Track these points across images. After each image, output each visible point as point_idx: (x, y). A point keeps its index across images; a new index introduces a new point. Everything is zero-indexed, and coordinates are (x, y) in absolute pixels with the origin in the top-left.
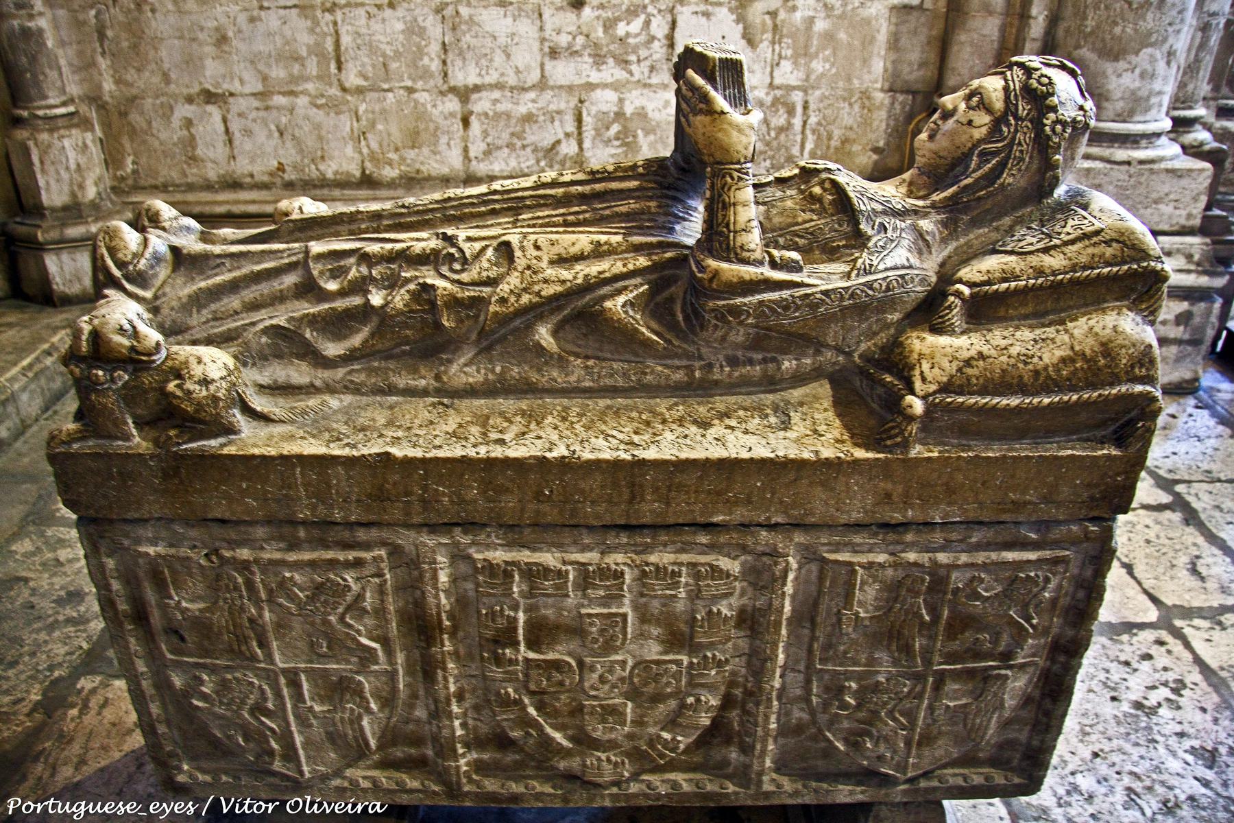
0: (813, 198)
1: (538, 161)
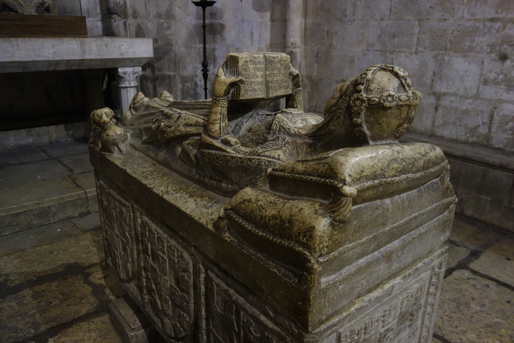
1: (466, 134)
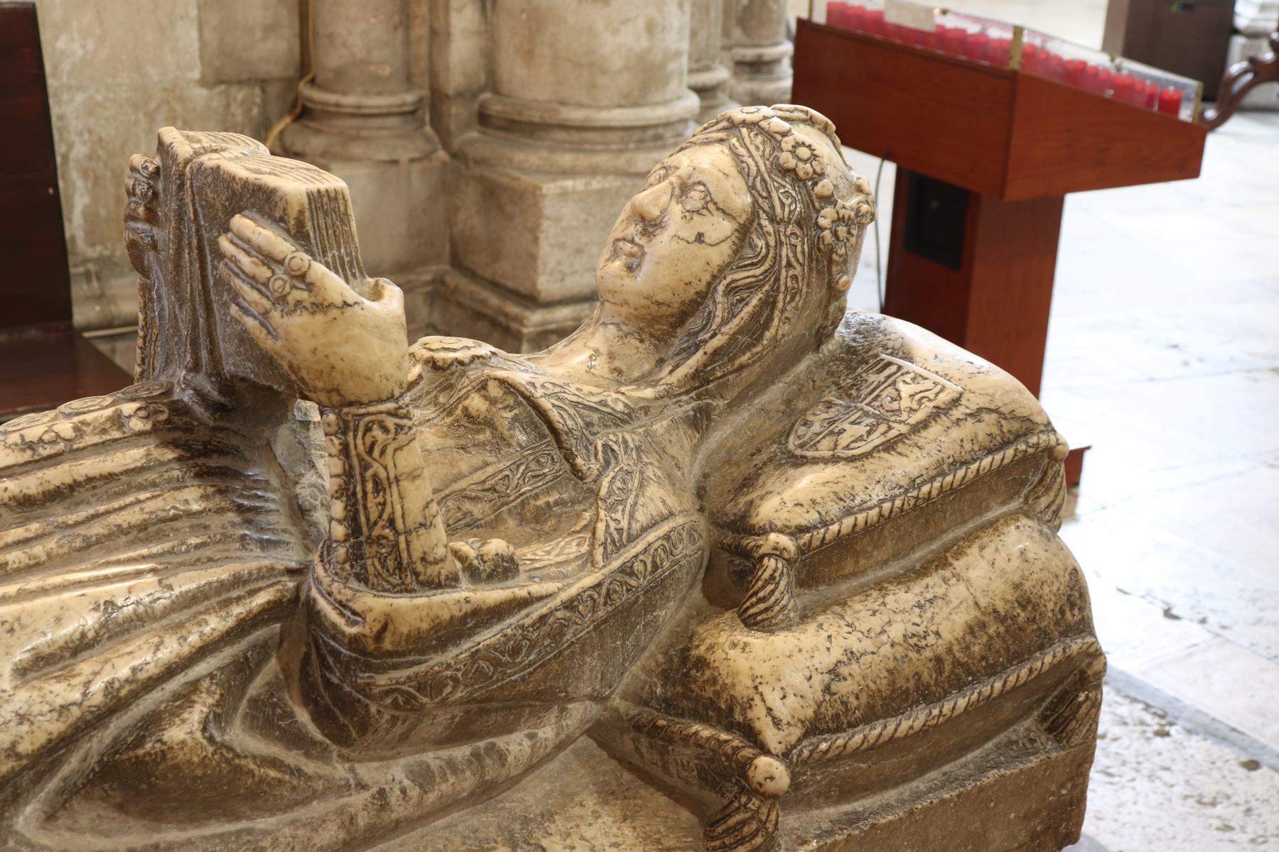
0: (473, 421)
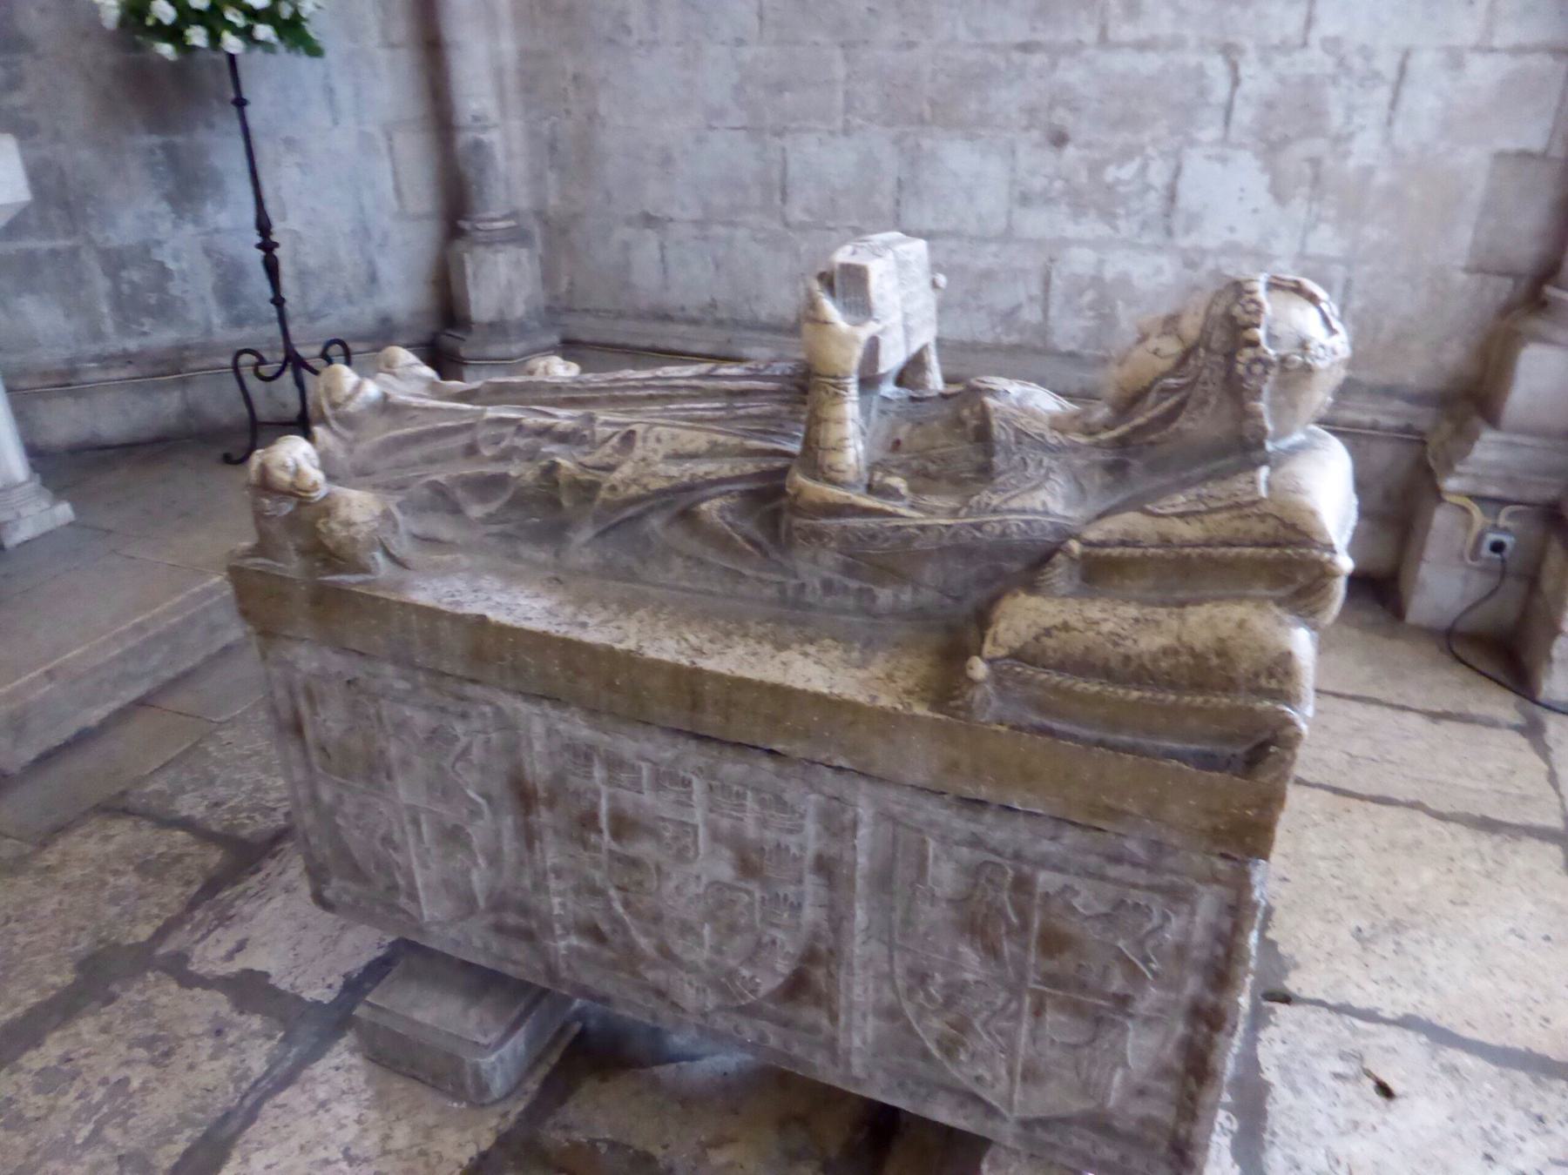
0: (960, 422)
1: (993, 327)
